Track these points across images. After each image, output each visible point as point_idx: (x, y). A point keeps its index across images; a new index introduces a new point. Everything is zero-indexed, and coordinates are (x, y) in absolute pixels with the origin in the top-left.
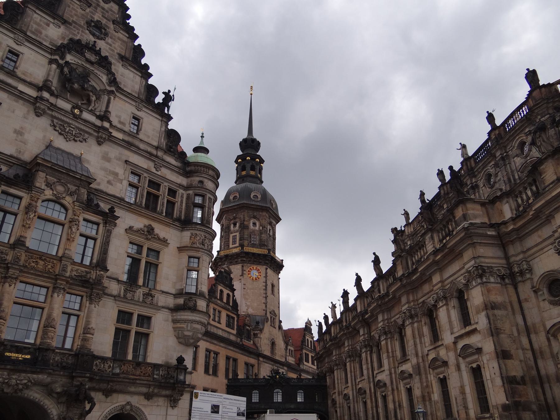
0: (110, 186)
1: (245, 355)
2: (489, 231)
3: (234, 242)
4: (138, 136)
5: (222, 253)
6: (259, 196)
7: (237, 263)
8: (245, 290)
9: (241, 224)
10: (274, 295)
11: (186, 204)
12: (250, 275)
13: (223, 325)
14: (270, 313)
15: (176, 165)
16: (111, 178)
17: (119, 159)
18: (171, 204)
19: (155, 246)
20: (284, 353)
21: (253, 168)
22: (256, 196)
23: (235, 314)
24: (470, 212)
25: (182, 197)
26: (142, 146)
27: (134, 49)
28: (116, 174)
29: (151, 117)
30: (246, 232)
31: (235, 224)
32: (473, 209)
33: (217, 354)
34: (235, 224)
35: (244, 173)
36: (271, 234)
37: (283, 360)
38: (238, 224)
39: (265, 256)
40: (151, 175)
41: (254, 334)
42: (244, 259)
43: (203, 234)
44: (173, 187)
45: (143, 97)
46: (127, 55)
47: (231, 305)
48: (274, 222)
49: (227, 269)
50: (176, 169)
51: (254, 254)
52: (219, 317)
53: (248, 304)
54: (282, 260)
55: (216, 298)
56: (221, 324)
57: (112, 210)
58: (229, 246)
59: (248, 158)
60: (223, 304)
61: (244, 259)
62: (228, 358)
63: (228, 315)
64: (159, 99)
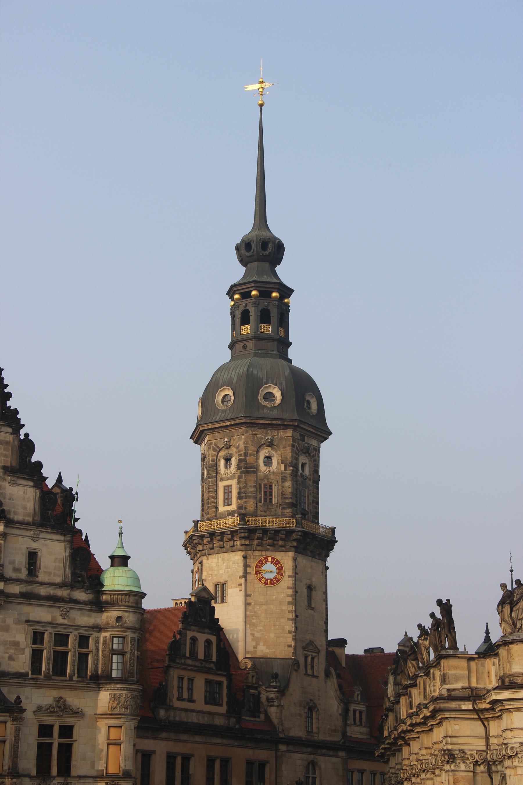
0: (12, 663)
1: (246, 747)
2: (464, 704)
3: (228, 501)
4: (37, 579)
5: (204, 527)
6: (278, 394)
7: (233, 549)
8: (250, 608)
9: (240, 461)
10: (313, 609)
11: (103, 651)
12: (259, 576)
13: (200, 704)
14: (304, 648)
15: (87, 599)
16: (12, 651)
17: (18, 622)
18: (83, 658)
19: (67, 721)
20: (339, 723)
21: (265, 317)
22: (269, 396)
23: (224, 675)
24: (451, 672)
25: (97, 642)
26: (43, 591)
27: (20, 447)
28: (16, 644)
29: (50, 543)
30: (251, 478)
31: (228, 460)
32: (456, 668)
33: (186, 759)
34: (228, 460)
35: (247, 330)
36: (307, 472)
37: (337, 738)
38: (234, 461)
39: (289, 532)
40: (56, 627)
41: (268, 699)
42: (247, 542)
43: (124, 693)
44: (85, 633)
45: (38, 518)
46: (14, 464)
47: (214, 659)
48: (314, 443)
49: (204, 595)
50: (88, 607)
51: (265, 531)
52: (190, 689)
53: (257, 635)
54: (333, 529)
55: (184, 656)
56: (194, 701)
57: (18, 700)
58: (217, 508)
59: (254, 293)
60: (197, 664)
61: (247, 542)
62: (211, 761)
63: (208, 682)
64: (59, 509)
